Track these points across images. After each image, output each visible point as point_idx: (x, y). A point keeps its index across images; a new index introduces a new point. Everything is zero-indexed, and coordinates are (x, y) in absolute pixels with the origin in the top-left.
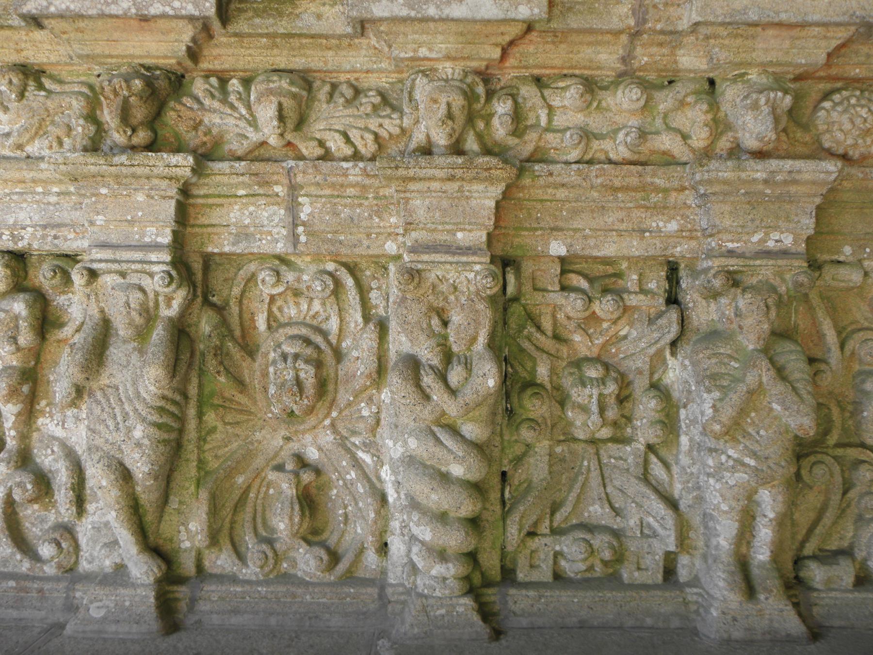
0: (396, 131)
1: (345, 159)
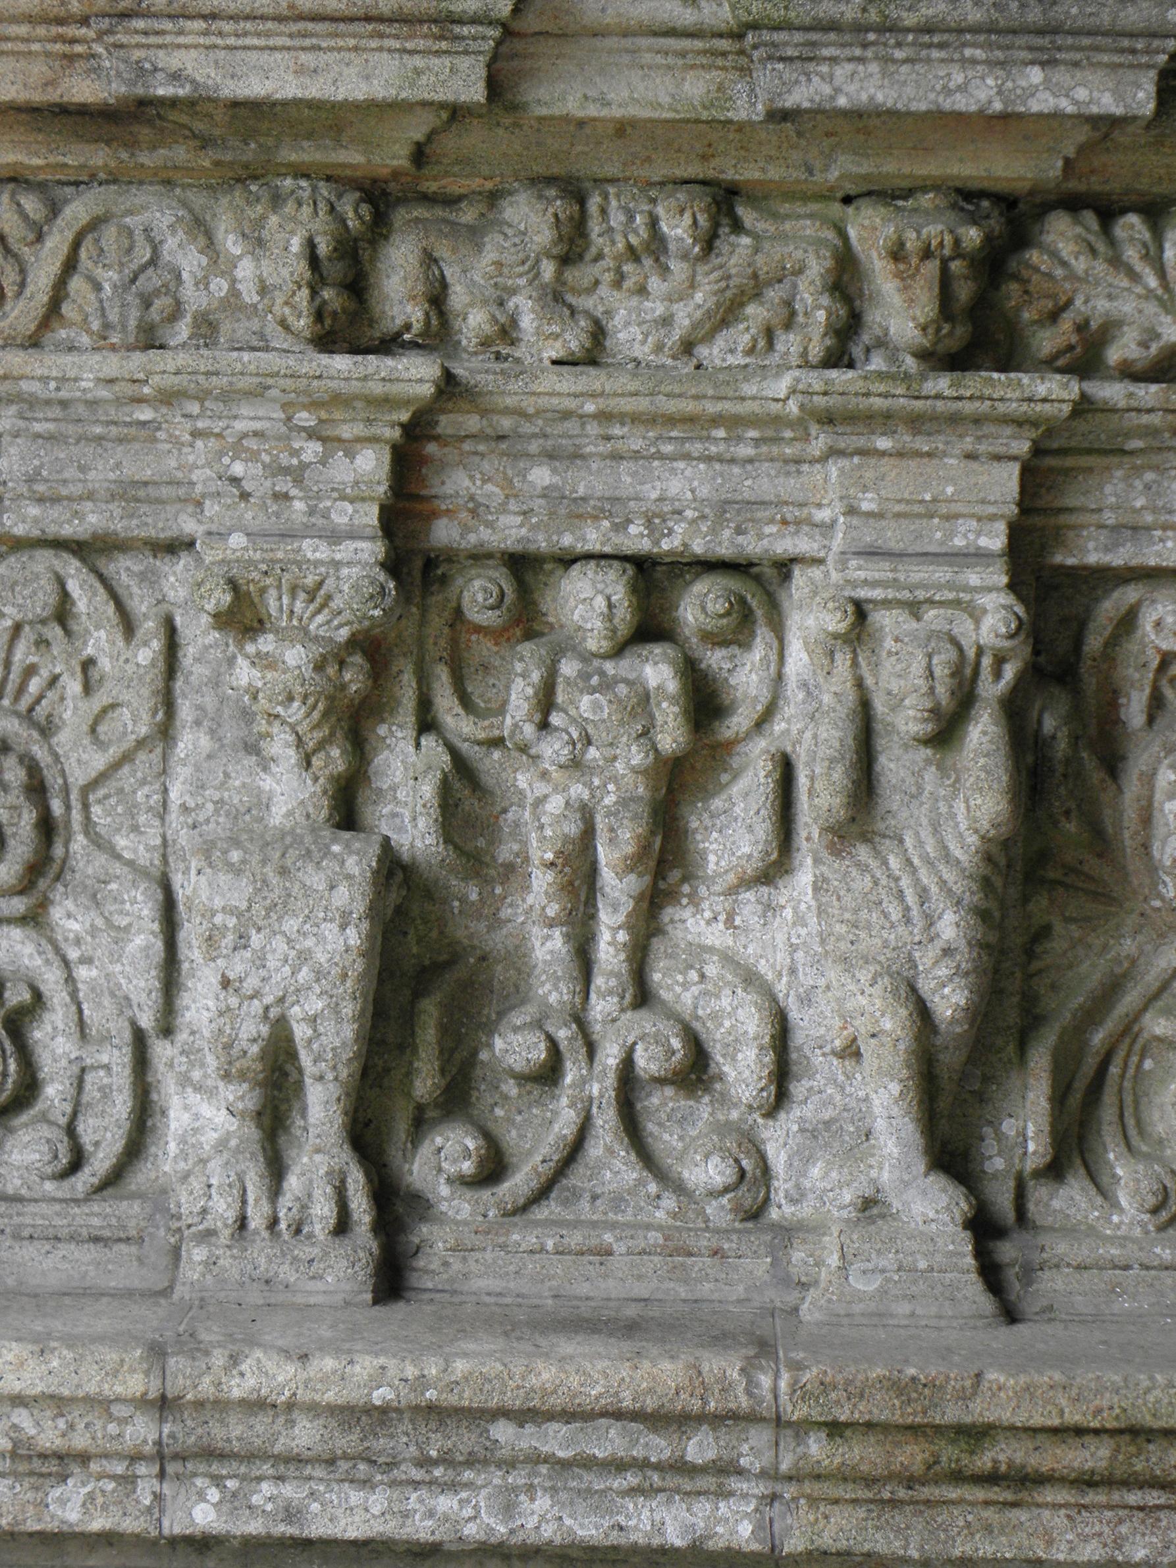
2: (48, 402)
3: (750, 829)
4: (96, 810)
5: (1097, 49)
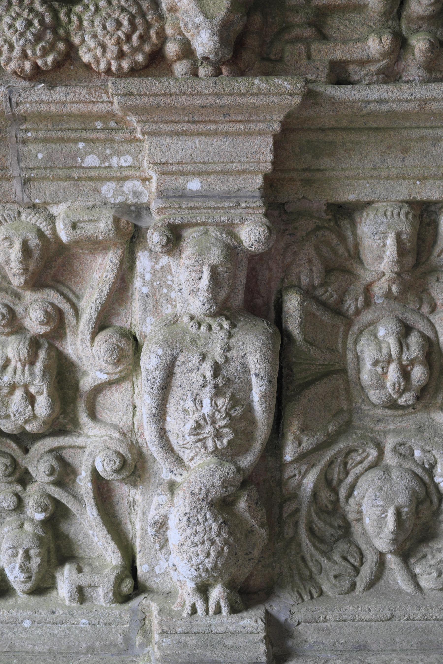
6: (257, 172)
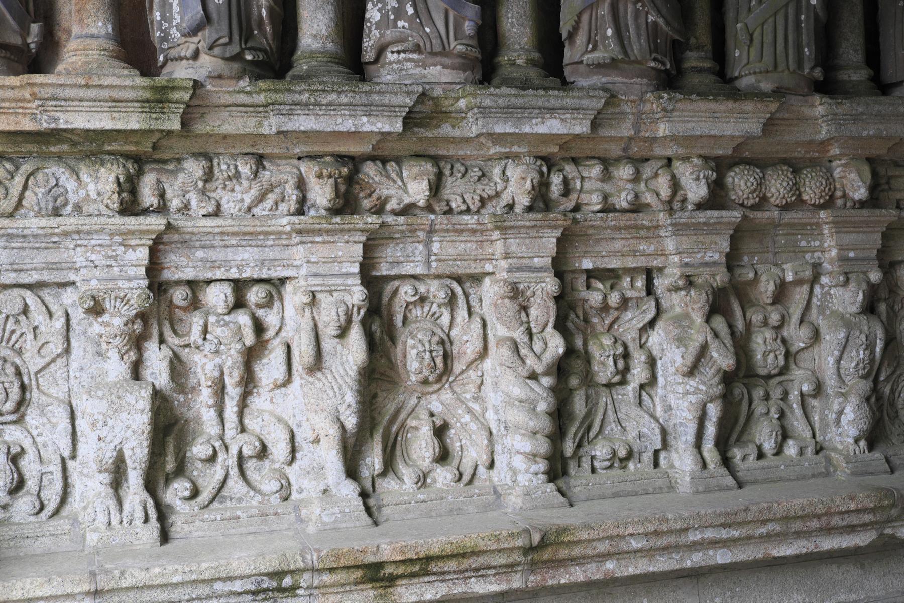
0: (492, 193)
1: (461, 212)
2: (18, 236)
3: (278, 369)
4: (41, 380)
5: (384, 111)
6: (874, 249)
